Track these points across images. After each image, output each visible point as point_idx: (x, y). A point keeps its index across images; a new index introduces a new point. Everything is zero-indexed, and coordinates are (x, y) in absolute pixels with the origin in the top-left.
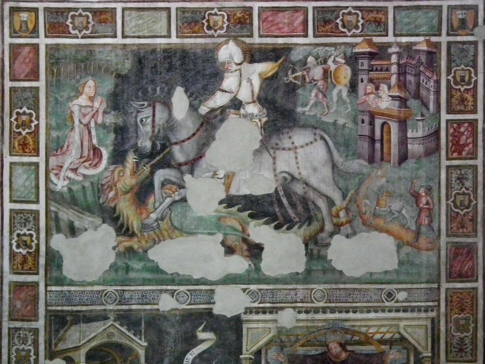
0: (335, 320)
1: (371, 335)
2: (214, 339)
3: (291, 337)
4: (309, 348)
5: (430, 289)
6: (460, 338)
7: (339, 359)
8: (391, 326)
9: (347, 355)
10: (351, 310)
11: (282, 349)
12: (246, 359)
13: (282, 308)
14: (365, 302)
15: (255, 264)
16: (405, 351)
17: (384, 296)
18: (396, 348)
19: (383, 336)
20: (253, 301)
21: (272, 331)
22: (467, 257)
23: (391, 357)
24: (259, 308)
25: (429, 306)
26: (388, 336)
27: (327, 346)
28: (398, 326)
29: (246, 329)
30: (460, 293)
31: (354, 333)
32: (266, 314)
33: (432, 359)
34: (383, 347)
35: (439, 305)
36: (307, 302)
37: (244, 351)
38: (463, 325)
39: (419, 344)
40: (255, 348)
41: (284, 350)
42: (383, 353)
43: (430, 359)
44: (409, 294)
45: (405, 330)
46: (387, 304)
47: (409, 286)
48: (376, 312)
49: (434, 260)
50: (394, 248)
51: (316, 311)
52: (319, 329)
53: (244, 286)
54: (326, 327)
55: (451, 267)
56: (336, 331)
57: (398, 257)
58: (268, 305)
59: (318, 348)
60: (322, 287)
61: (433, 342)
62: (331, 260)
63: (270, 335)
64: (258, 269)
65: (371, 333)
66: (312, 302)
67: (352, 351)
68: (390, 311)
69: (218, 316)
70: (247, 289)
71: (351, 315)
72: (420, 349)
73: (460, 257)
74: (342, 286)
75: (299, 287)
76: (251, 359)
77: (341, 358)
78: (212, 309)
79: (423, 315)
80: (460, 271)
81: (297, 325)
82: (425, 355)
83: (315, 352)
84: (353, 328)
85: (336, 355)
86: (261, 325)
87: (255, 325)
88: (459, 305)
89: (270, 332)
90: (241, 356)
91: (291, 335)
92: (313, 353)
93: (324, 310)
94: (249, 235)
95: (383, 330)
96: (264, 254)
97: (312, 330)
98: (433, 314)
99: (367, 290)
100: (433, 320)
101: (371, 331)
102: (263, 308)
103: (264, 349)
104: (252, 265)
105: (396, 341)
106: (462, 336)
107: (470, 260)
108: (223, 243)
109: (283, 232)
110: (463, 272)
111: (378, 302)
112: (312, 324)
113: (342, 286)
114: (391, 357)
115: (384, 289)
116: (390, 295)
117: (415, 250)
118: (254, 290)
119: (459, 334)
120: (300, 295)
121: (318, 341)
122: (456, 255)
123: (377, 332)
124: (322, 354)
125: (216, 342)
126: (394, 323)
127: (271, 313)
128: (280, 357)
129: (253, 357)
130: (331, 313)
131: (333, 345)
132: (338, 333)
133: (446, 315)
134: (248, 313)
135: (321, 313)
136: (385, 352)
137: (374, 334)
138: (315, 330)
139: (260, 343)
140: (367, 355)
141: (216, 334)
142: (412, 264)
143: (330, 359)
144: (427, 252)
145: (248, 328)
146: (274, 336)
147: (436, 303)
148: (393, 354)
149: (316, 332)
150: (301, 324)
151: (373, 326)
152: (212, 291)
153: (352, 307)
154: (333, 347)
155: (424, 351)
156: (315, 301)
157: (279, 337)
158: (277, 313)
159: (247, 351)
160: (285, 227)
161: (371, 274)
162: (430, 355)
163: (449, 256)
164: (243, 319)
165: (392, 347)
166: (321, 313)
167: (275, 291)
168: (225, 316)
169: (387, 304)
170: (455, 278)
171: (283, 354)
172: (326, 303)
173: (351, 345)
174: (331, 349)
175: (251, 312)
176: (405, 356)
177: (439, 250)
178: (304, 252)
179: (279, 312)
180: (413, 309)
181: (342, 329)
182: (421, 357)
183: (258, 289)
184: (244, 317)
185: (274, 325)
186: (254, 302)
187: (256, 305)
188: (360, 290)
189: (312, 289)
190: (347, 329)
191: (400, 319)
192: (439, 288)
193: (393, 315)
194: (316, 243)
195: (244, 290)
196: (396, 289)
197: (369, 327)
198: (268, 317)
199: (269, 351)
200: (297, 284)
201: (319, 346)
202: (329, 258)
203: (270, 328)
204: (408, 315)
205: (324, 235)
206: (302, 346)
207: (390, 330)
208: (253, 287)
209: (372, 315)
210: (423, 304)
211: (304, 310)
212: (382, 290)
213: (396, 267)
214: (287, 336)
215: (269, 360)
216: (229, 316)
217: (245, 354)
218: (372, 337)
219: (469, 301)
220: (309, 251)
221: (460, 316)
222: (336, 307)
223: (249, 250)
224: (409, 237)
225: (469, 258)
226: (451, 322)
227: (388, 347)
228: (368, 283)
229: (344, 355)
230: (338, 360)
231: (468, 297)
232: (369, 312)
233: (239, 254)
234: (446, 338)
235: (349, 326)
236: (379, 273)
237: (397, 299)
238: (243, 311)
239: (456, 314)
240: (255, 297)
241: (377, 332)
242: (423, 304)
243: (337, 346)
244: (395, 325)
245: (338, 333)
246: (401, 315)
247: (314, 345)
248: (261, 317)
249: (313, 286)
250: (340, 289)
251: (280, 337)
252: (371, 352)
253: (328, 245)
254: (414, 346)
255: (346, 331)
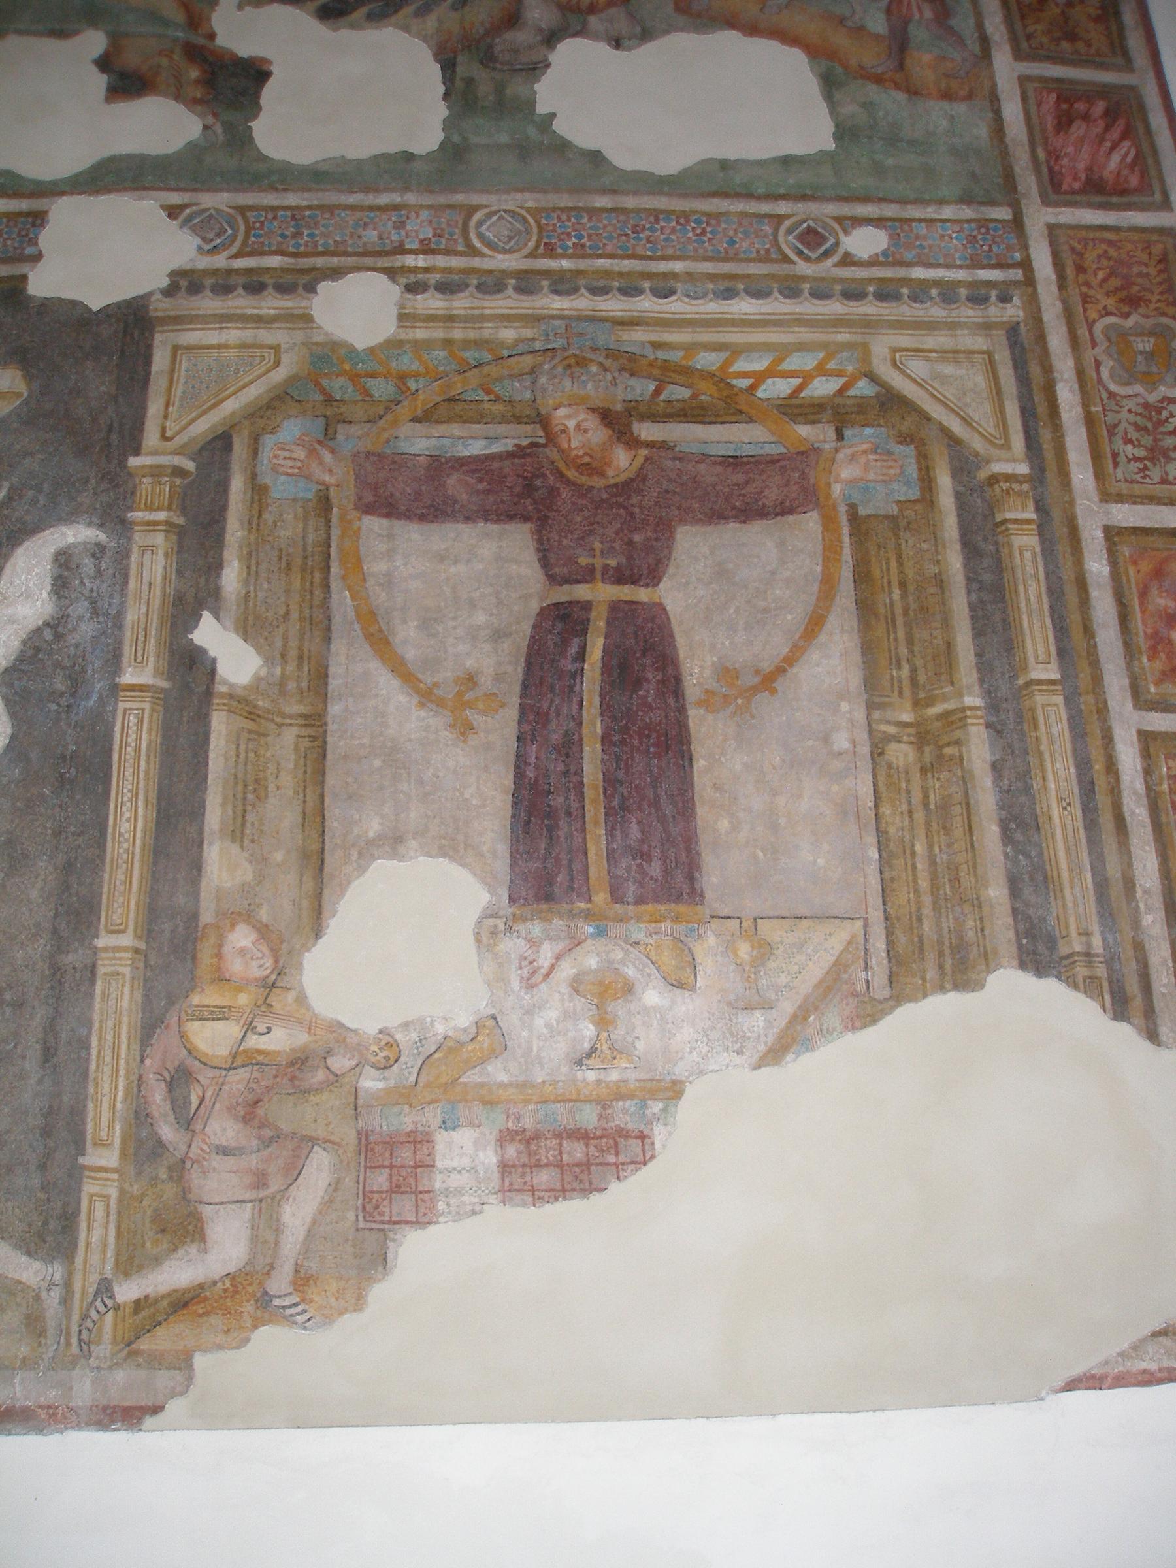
0: (579, 318)
1: (744, 383)
2: (19, 395)
3: (371, 383)
4: (456, 429)
5: (983, 223)
6: (1146, 406)
7: (602, 474)
8: (831, 350)
9: (639, 461)
10: (647, 285)
11: (329, 433)
12: (156, 472)
13: (335, 274)
14: (706, 259)
15: (229, 127)
16: (910, 450)
17: (788, 242)
18: (862, 437)
19: (800, 388)
20: (207, 247)
21: (285, 359)
22: (1107, 128)
23: (846, 473)
24: (229, 272)
25: (989, 284)
26: (822, 388)
27: (543, 421)
28: (865, 348)
29: (168, 354)
30: (1110, 243)
31: (666, 373)
32: (265, 293)
33: (1034, 488)
34: (804, 430)
35: (1030, 281)
36: (448, 252)
37: (151, 438)
38: (1150, 356)
39: (966, 421)
40: (203, 427)
41: (340, 437)
42: (807, 454)
43: (1025, 487)
44: (894, 237)
45: (894, 364)
46: (803, 268)
47: (890, 210)
48: (758, 294)
49: (982, 131)
50: (811, 85)
51: (493, 284)
52: (500, 355)
53: (175, 198)
54: (538, 345)
55: (1054, 155)
56: (582, 362)
57: (833, 111)
58: (275, 261)
59: (502, 429)
60: (511, 201)
61: (1028, 414)
62: (553, 116)
63: (280, 375)
64: (240, 140)
65: (745, 375)
66: (473, 252)
67: (663, 446)
68: (820, 294)
69: (46, 306)
70: (183, 207)
71: (646, 304)
72: (978, 444)
73: (1078, 129)
74: (601, 202)
75: (411, 198)
76: (178, 472)
77: (610, 473)
78: (24, 278)
79: (969, 314)
80: (1089, 169)
81: (403, 335)
82: (998, 468)
83: (486, 447)
84: (660, 354)
85: (587, 459)
86: (233, 335)
87: (212, 337)
88: (1115, 282)
89: (277, 364)
90: (134, 462)
91: (373, 375)
92: (476, 448)
93: (526, 282)
94: (212, 36)
95: (795, 362)
96: (269, 93)
97: (470, 355)
98: (1014, 311)
99: (718, 216)
100: (1013, 331)
101: (741, 365)
102: (249, 271)
103: (246, 432)
104: (219, 129)
105: (862, 406)
106: (1152, 398)
107: (1125, 136)
108: (104, 63)
109: (352, 27)
110: (1106, 174)
111: (765, 259)
112: (472, 335)
113: (601, 202)
114: (846, 473)
115: (787, 217)
116: (811, 237)
117: (901, 96)
118: (217, 210)
119: (1138, 388)
120: (420, 228)
121: (498, 399)
122: (1064, 122)
123: (770, 373)
124: (519, 453)
125: (26, 402)
126: (843, 337)
127: (284, 289)
128: (321, 463)
129: (190, 466)
130: (556, 292)
131: (568, 417)
132: (594, 369)
133: (1069, 316)
134: (183, 293)
135: (510, 291)
136: (817, 450)
137: (759, 378)
138: (487, 356)
139: (231, 406)
140: (734, 462)
141: (29, 378)
142: (893, 140)
143: (561, 475)
144: (945, 104)
145: (176, 348)
146: (292, 380)
147: (1017, 274)
148: (853, 458)
149: (488, 363)
150: (420, 334)
151: (750, 348)
152: (38, 219)
153: (649, 276)
154: (571, 424)
155: (995, 452)
156: (486, 250)
157: (317, 384)
158: (311, 289)
159: (164, 438)
160: (364, 10)
161: (725, 165)
162: (1023, 469)
163: (1035, 120)
164: (159, 314)
165: (848, 433)
166: (510, 291)
167: (308, 213)
168: (74, 304)
169: (803, 268)
170: (1074, 193)
171: (333, 452)
172: (532, 255)
173: (654, 417)
174: (563, 431)
175: (195, 288)
176: (912, 471)
177: (994, 99)
178: (442, 89)
179: (323, 287)
180: (919, 293)
181: (612, 354)
182: (982, 475)
183: (236, 208)
184: (160, 307)
185: (299, 336)
186: (214, 251)
187: (220, 261)
188: (683, 217)
189: (476, 209)
190: (632, 357)
191: (869, 324)
192: (1018, 223)
193: (836, 307)
194: (488, 59)
195: (173, 212)
196: (839, 220)
197: (736, 352)
198: (270, 304)
199: (268, 441)
200: (407, 189)
201: (503, 420)
202: (542, 109)
203: (276, 348)
204: (906, 310)
205: (521, 37)
206: (425, 417)
207: (832, 365)
208: (217, 201)
209: (744, 307)
210: (960, 275)
211: (437, 277)
212: (780, 219)
213: (831, 146)
214: (354, 378)
215: (266, 479)
216: (96, 304)
217: (155, 453)
218: (753, 388)
219: (1153, 271)
220: (459, 84)
221: (1130, 322)
222: (579, 272)
223: (210, 81)
224: (871, 57)
225: (1115, 134)
226: (1094, 345)
227: (831, 434)
228: (714, 194)
229: (623, 461)
230: (597, 482)
231: (1144, 257)
232: (729, 294)
233: (165, 95)
234: (1086, 404)
235: (643, 343)
236: (760, 163)
237: (847, 254)
238: (165, 282)
239: (1109, 314)
240: (218, 235)
241: (770, 373)
242: (960, 275)
243: (592, 422)
244: (849, 346)
245: (594, 369)
246: (869, 308)
247: (481, 418)
248: (240, 303)
249: (476, 199)
250: (593, 212)
251: (325, 382)
252: (747, 450)
253: (537, 69)
254: (945, 431)
255: (630, 364)
